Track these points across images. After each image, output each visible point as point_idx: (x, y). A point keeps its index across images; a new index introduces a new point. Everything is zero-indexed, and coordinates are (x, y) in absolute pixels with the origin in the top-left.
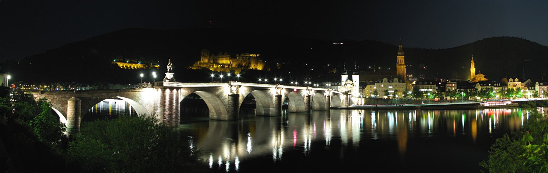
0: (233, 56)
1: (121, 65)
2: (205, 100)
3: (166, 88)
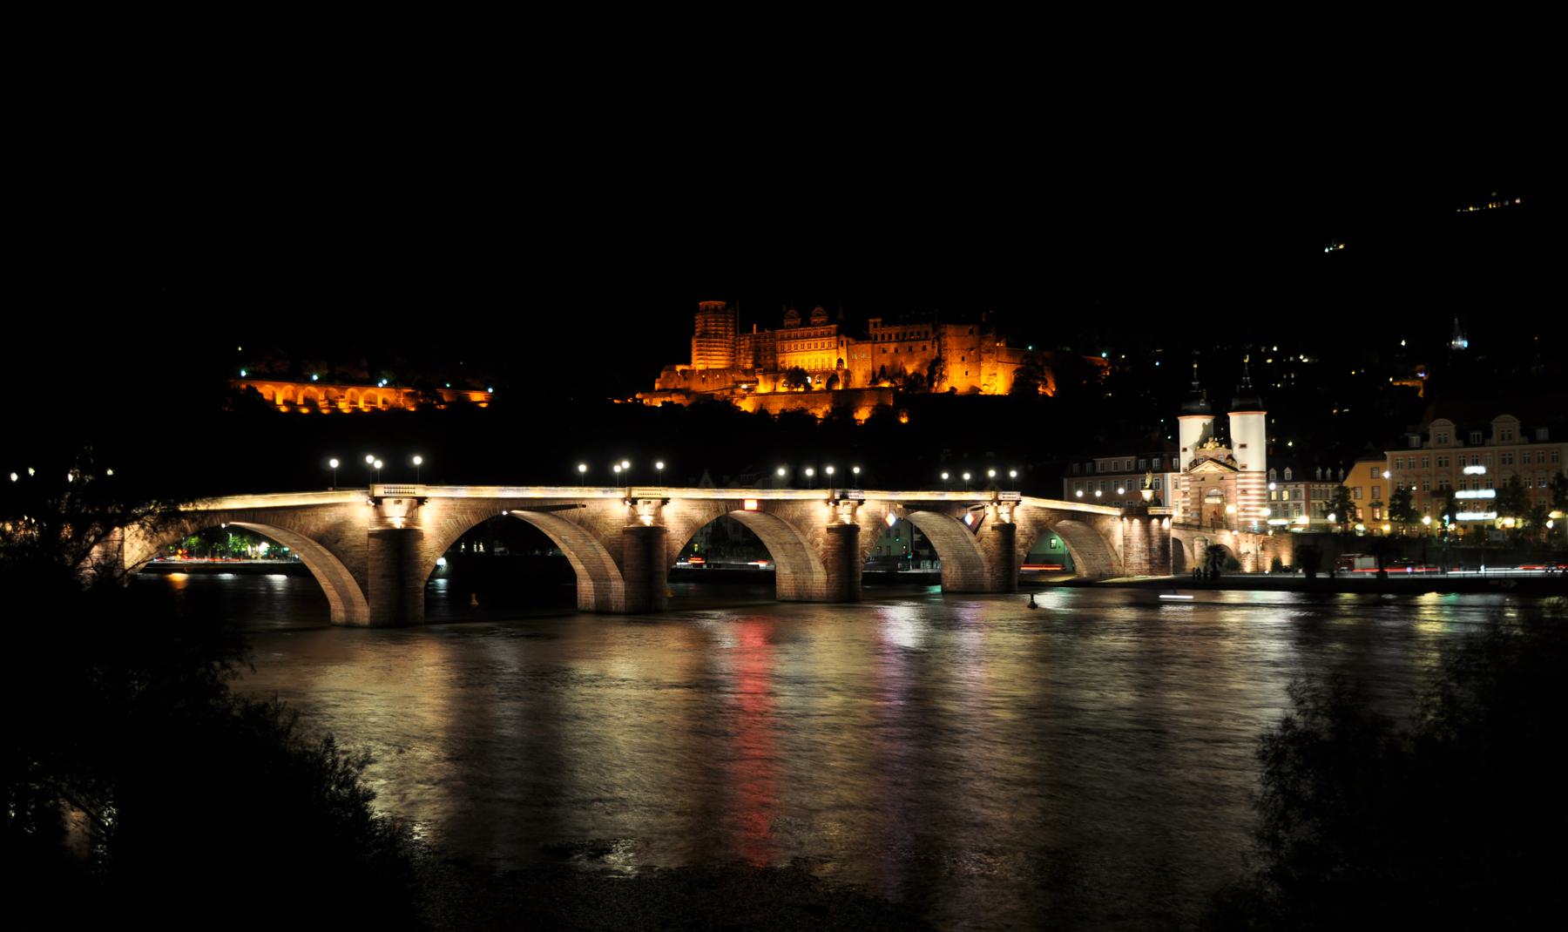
0: (852, 331)
1: (279, 394)
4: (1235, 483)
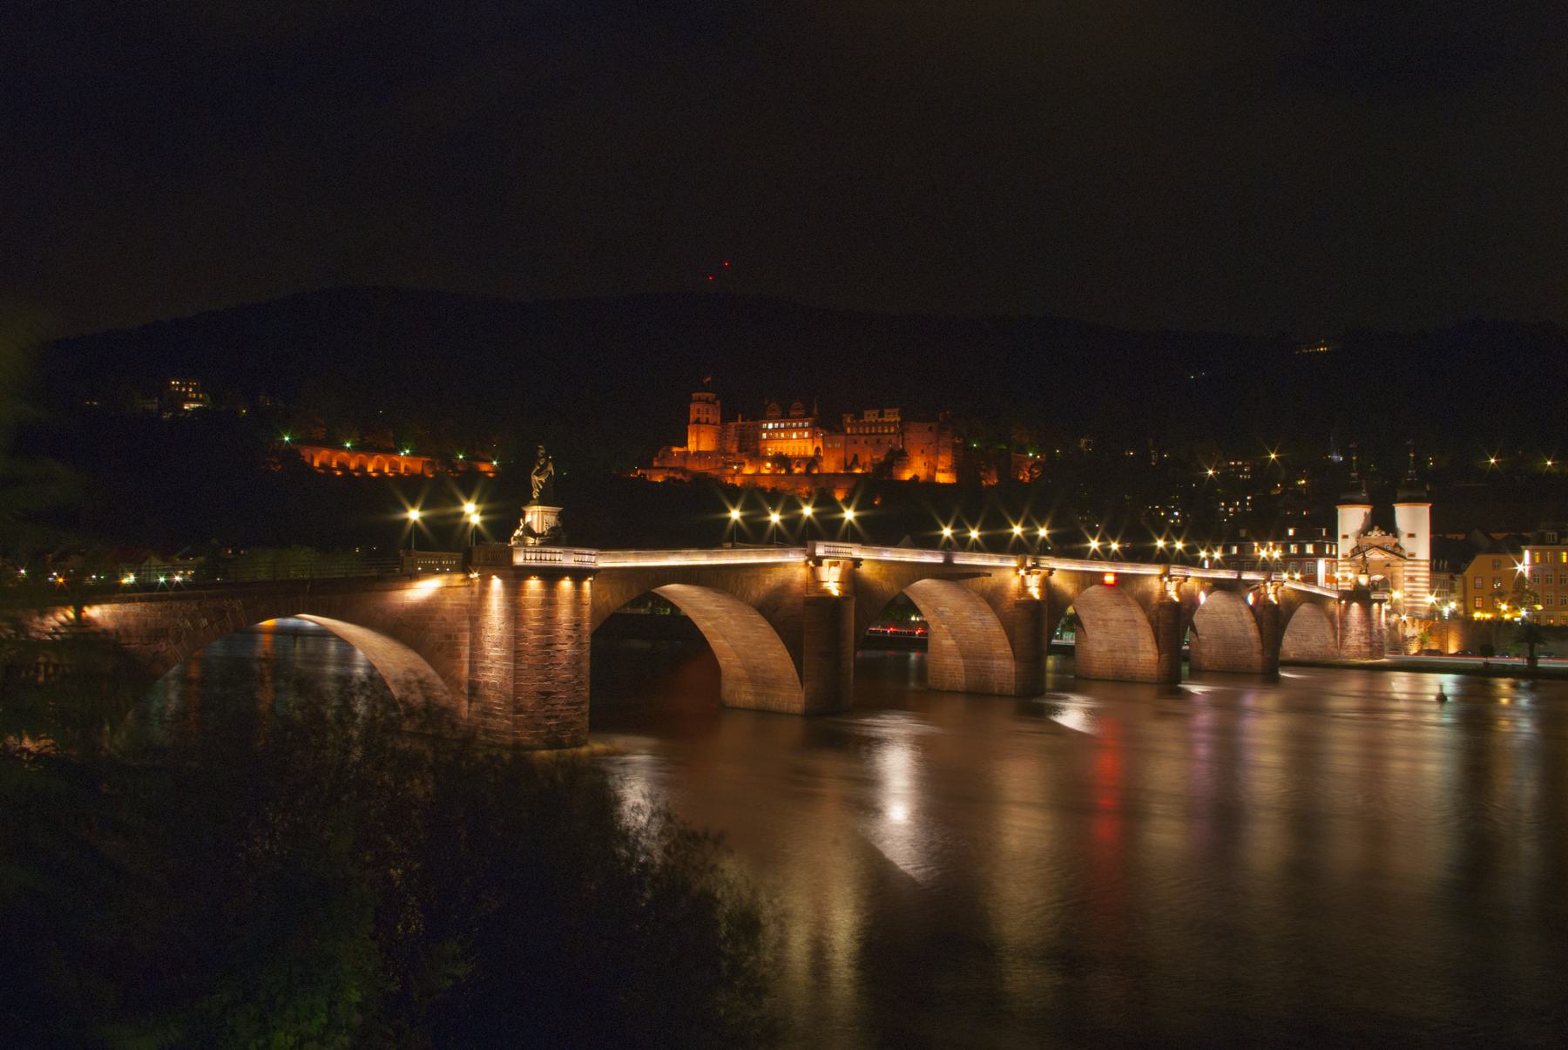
0: (826, 423)
2: (704, 625)
3: (526, 572)
4: (1402, 571)
